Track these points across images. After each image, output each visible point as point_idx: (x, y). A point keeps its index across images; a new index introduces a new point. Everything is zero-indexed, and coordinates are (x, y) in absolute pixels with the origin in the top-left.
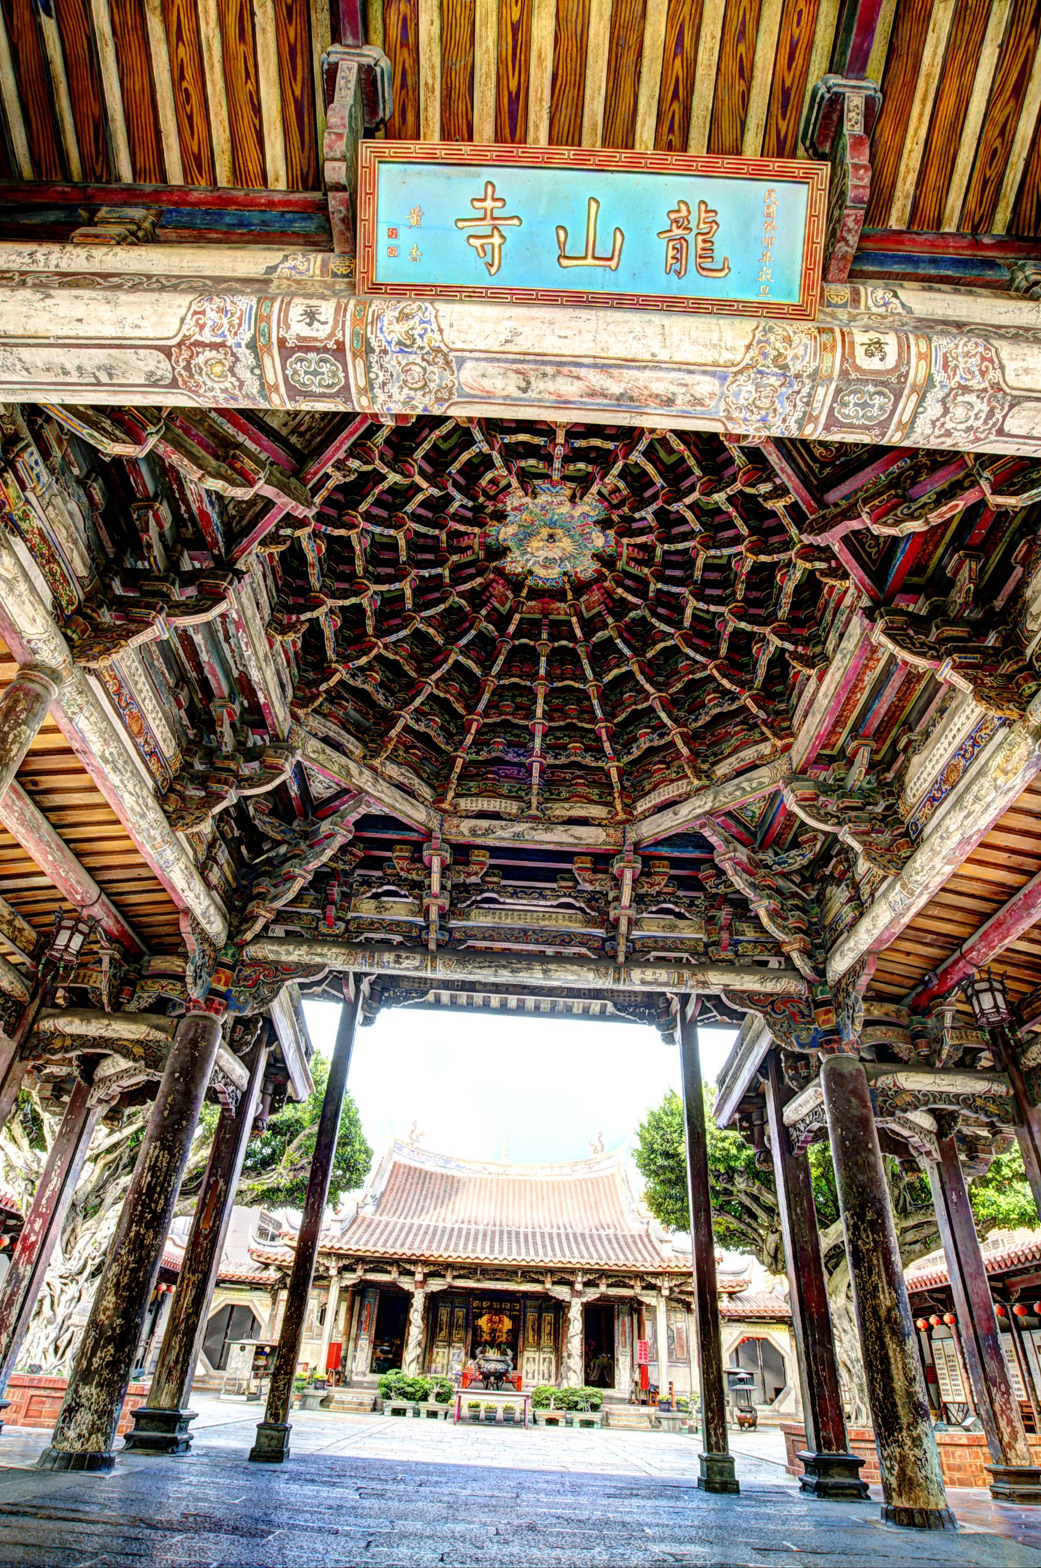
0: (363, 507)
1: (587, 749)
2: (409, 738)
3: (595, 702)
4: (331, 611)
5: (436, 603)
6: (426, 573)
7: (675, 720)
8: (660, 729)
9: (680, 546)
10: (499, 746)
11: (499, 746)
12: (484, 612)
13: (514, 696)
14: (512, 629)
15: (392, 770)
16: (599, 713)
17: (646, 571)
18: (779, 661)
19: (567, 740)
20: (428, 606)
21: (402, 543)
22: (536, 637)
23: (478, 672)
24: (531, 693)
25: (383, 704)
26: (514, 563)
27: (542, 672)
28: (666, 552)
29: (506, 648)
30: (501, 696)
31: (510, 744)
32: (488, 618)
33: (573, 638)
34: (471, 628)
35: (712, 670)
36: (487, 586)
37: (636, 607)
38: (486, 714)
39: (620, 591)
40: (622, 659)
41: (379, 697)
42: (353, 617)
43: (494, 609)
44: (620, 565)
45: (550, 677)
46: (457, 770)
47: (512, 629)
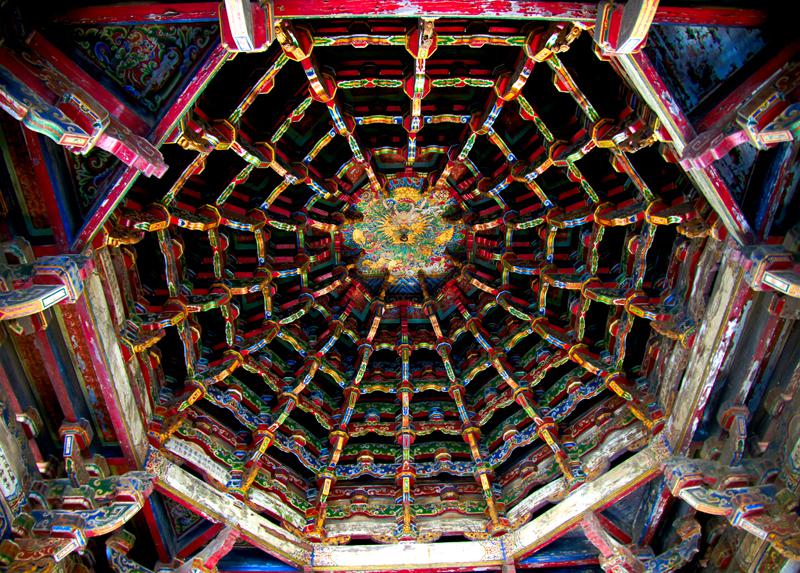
0: (221, 200)
1: (455, 458)
2: (272, 462)
3: (460, 404)
4: (190, 321)
5: (296, 309)
6: (282, 274)
7: (541, 415)
8: (526, 424)
9: (532, 224)
10: (366, 464)
11: (366, 464)
12: (343, 317)
13: (379, 408)
14: (372, 334)
15: (259, 498)
16: (464, 417)
17: (498, 257)
18: (642, 328)
19: (432, 450)
20: (286, 314)
21: (260, 243)
22: (397, 341)
23: (341, 382)
24: (394, 399)
25: (248, 424)
26: (372, 266)
27: (406, 377)
28: (517, 235)
29: (367, 354)
30: (364, 408)
31: (378, 460)
32: (348, 324)
33: (432, 338)
34: (332, 334)
35: (573, 354)
36: (344, 291)
37: (489, 297)
38: (350, 428)
39: (475, 282)
40: (480, 354)
41: (243, 417)
42: (211, 324)
43: (351, 315)
44: (471, 255)
45: (412, 383)
46: (326, 491)
47: (372, 334)
